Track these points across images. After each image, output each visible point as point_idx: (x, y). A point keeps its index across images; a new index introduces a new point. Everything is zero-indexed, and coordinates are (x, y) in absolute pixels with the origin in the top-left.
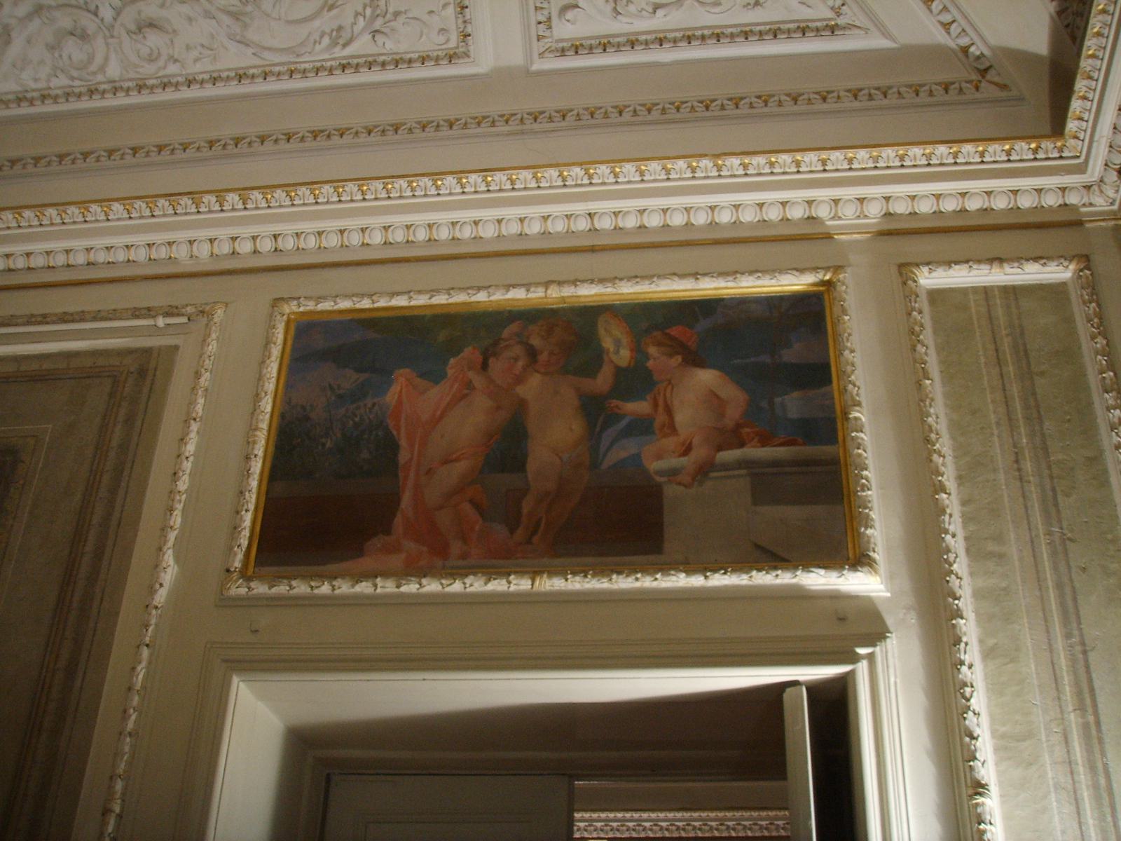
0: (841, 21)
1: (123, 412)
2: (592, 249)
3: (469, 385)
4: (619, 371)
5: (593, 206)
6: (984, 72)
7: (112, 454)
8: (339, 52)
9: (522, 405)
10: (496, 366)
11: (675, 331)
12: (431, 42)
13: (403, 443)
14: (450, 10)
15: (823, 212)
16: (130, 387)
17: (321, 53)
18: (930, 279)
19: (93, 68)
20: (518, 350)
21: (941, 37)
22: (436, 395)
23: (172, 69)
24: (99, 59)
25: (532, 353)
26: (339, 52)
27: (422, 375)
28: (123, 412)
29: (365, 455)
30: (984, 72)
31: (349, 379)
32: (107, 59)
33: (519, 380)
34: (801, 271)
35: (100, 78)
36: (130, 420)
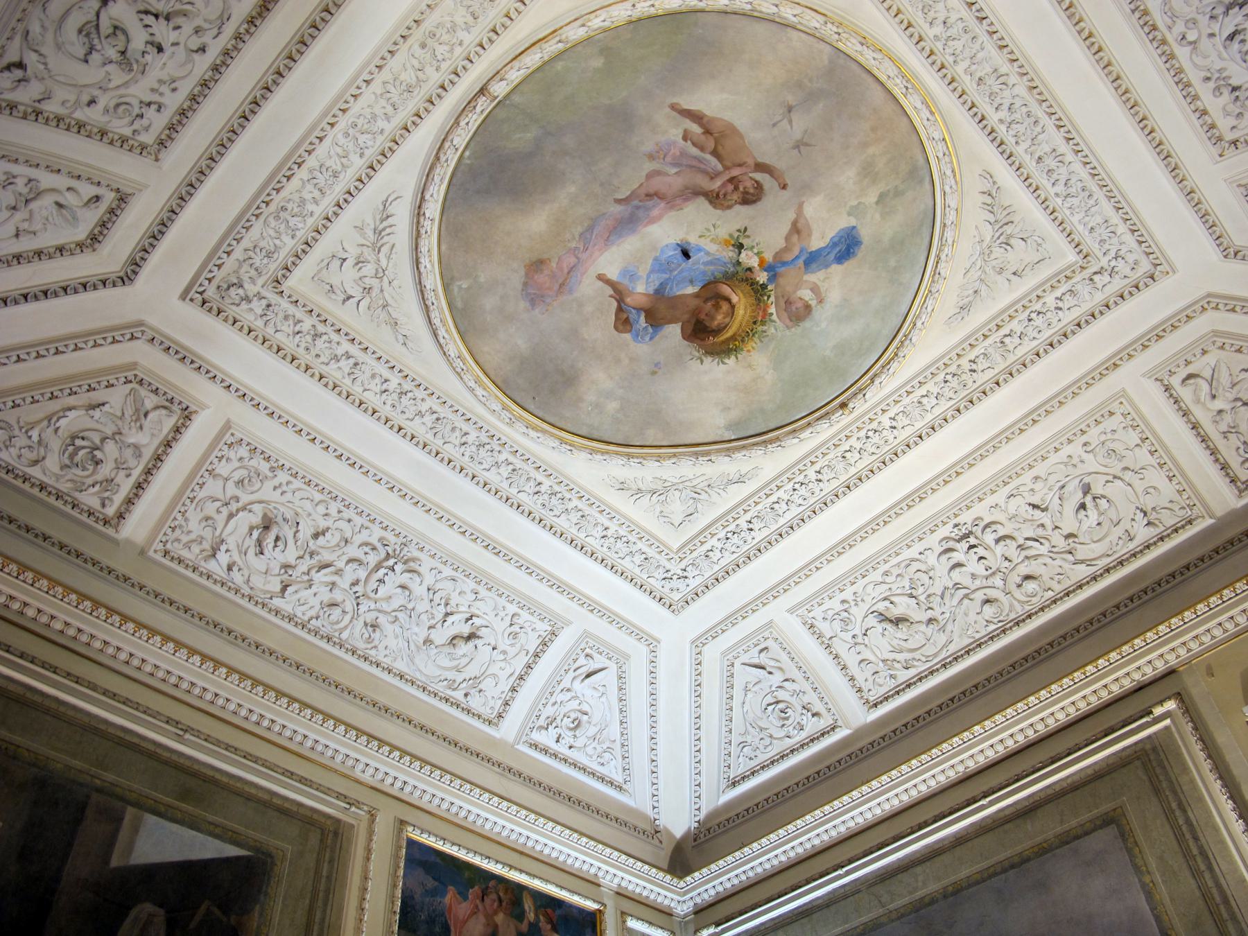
0: (624, 786)
1: (327, 855)
2: (522, 853)
3: (477, 907)
4: (530, 924)
5: (530, 834)
6: (657, 832)
7: (323, 880)
8: (449, 692)
9: (496, 926)
10: (487, 901)
11: (549, 911)
12: (486, 712)
13: (452, 928)
14: (500, 702)
15: (601, 874)
16: (328, 839)
17: (440, 687)
18: (632, 924)
19: (336, 627)
20: (494, 896)
21: (651, 813)
22: (463, 909)
23: (373, 652)
24: (342, 625)
25: (500, 901)
26: (449, 692)
27: (459, 893)
28: (327, 855)
29: (437, 929)
30: (657, 832)
31: (431, 883)
32: (346, 627)
33: (496, 913)
34: (594, 901)
35: (337, 634)
36: (331, 861)
